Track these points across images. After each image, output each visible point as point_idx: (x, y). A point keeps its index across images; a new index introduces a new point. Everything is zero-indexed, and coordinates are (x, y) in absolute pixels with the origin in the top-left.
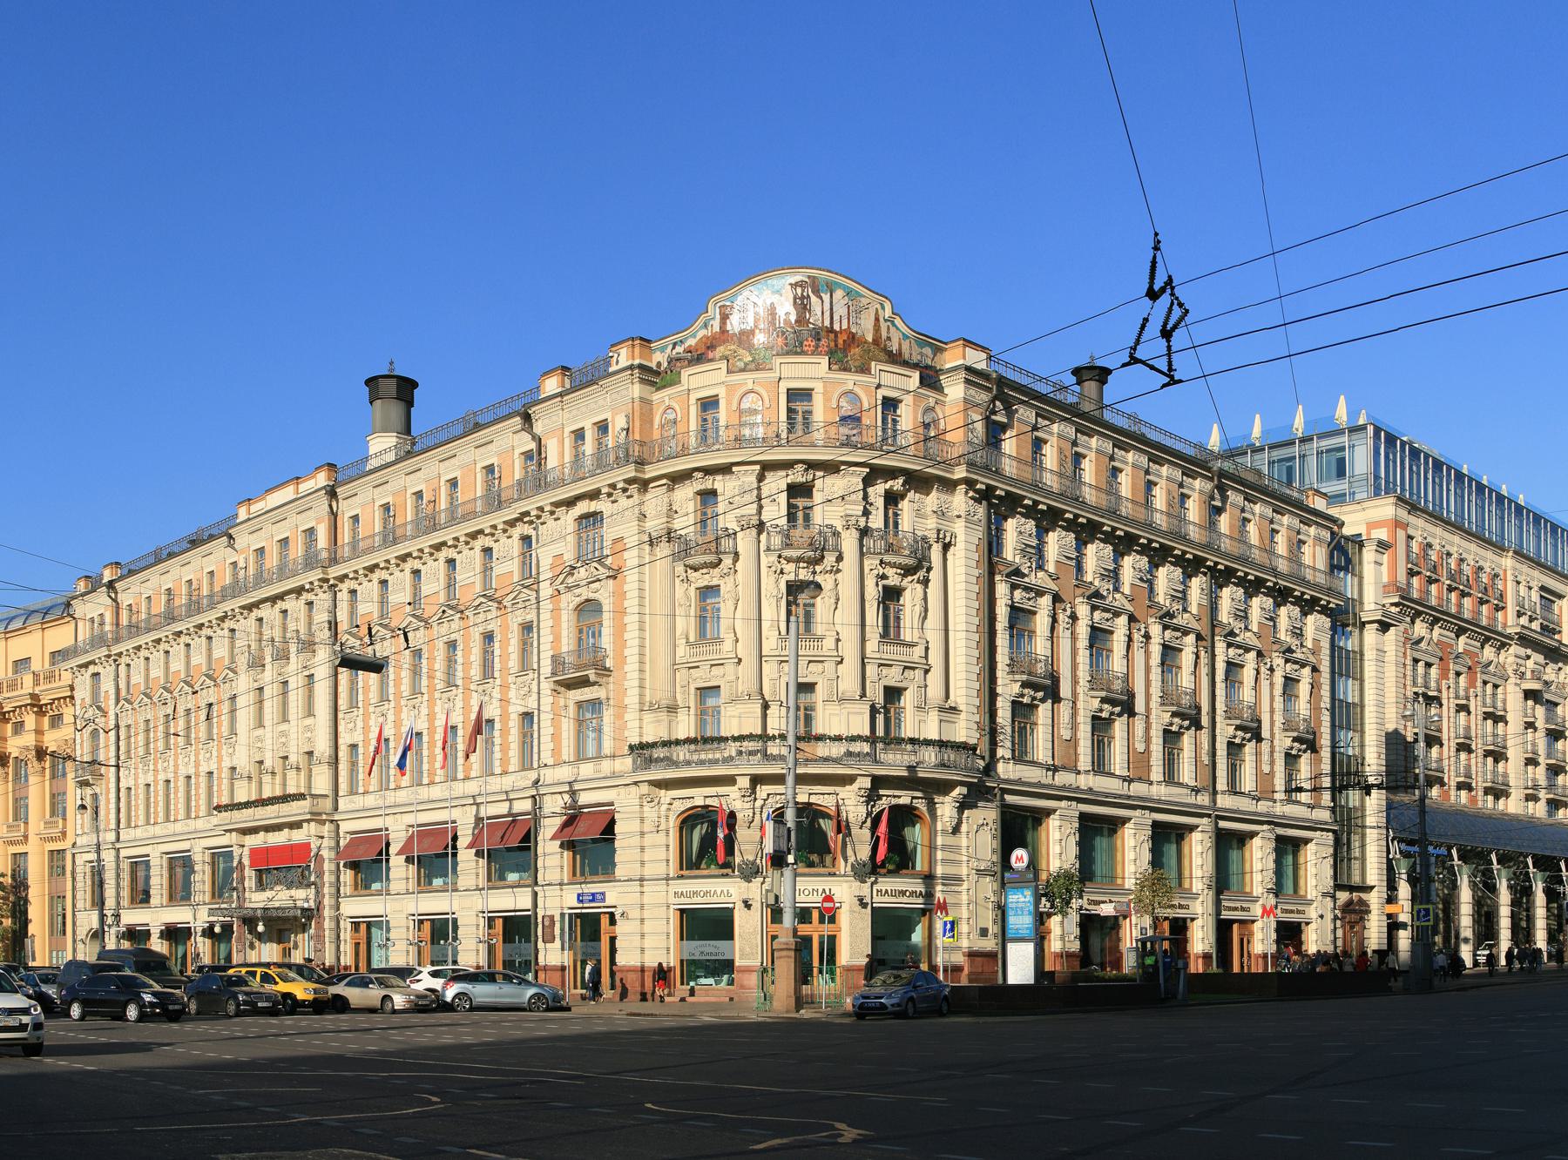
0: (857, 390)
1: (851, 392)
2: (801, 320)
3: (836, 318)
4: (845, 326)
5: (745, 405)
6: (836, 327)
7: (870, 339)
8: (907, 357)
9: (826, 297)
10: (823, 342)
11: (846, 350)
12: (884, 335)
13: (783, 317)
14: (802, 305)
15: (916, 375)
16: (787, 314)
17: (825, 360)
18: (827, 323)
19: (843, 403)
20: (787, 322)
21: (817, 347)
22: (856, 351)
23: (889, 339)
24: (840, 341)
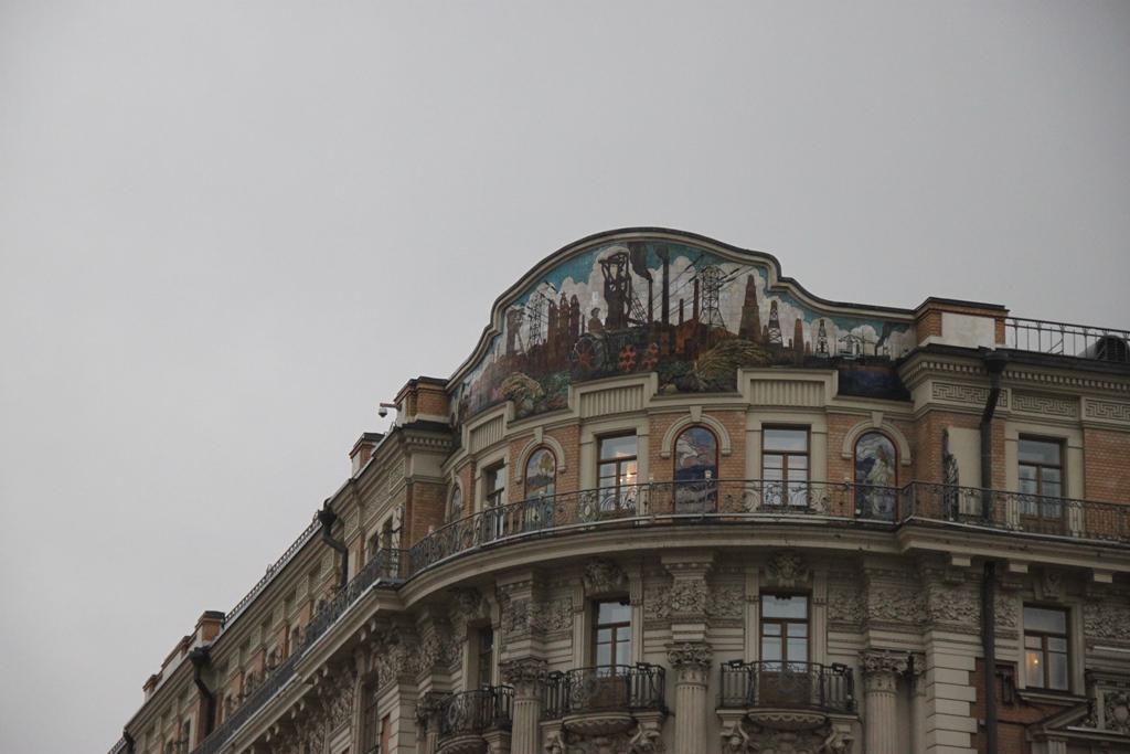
0: (711, 420)
1: (697, 425)
2: (617, 318)
3: (673, 305)
4: (688, 316)
5: (531, 473)
6: (674, 320)
7: (734, 328)
8: (814, 348)
9: (658, 275)
10: (652, 349)
11: (689, 354)
12: (764, 319)
13: (589, 317)
14: (617, 294)
15: (832, 381)
16: (595, 311)
17: (651, 383)
18: (657, 316)
19: (685, 447)
20: (595, 323)
21: (639, 358)
22: (708, 356)
23: (774, 323)
24: (680, 342)
